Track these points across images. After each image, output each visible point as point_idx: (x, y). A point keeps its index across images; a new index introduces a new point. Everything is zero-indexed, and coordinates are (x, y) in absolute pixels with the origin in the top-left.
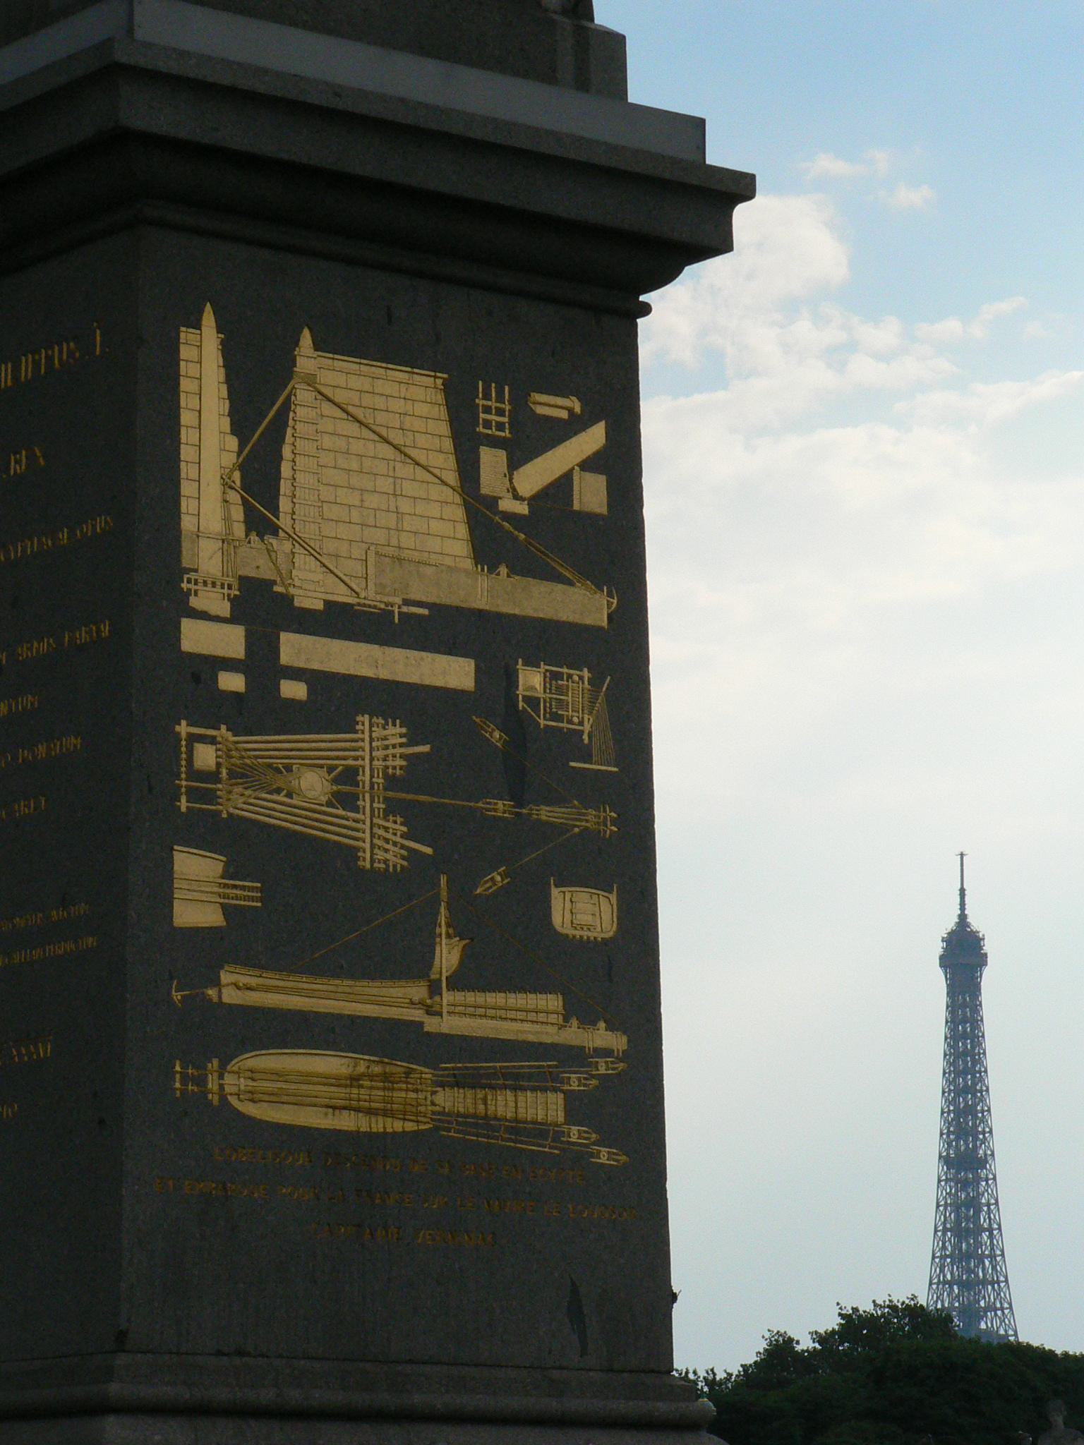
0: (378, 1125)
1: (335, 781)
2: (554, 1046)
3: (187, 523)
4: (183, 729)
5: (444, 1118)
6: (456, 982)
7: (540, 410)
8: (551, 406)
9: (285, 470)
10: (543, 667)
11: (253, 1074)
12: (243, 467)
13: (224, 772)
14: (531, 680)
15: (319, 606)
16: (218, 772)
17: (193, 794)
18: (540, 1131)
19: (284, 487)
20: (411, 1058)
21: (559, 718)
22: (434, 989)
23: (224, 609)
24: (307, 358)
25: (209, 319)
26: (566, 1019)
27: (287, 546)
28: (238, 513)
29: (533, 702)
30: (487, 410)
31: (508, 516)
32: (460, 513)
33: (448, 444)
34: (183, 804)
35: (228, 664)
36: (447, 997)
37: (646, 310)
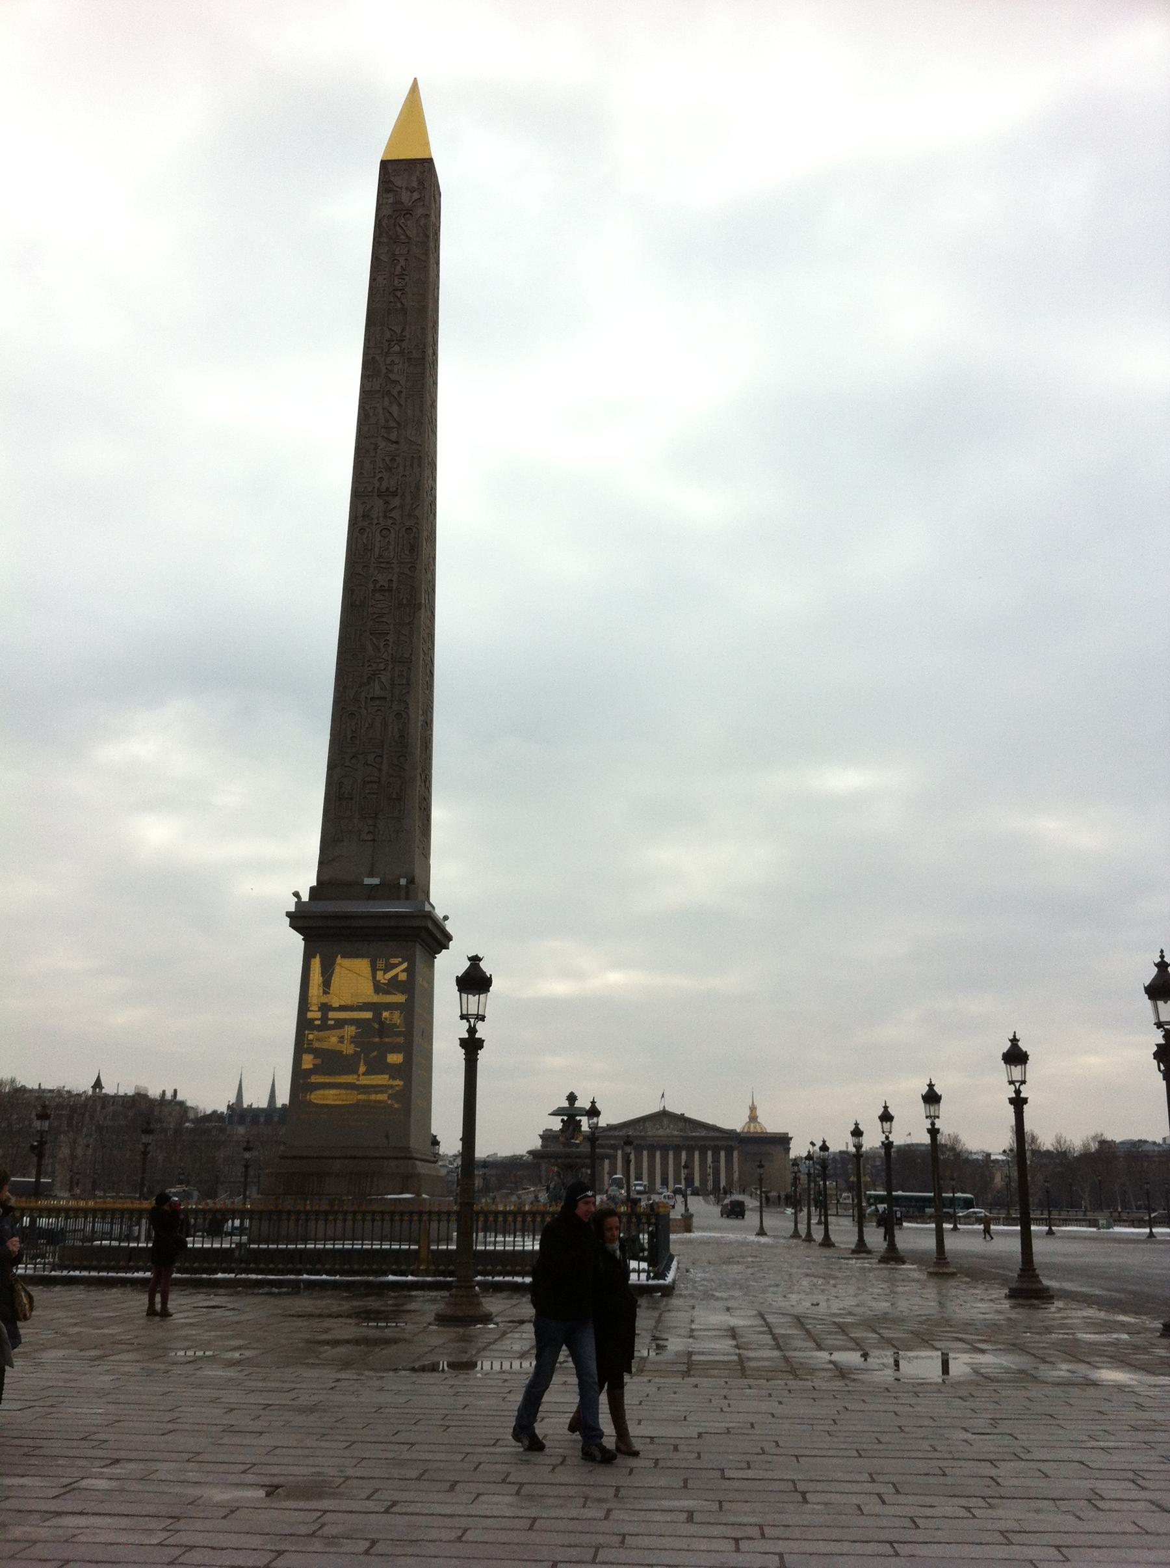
0: (344, 1103)
3: (310, 995)
4: (306, 1032)
5: (359, 1101)
6: (363, 1074)
8: (394, 961)
12: (323, 982)
14: (385, 1014)
18: (380, 1102)
22: (359, 1076)
23: (317, 1009)
24: (339, 960)
25: (318, 955)
28: (321, 991)
29: (386, 1019)
33: (370, 972)
36: (361, 1077)
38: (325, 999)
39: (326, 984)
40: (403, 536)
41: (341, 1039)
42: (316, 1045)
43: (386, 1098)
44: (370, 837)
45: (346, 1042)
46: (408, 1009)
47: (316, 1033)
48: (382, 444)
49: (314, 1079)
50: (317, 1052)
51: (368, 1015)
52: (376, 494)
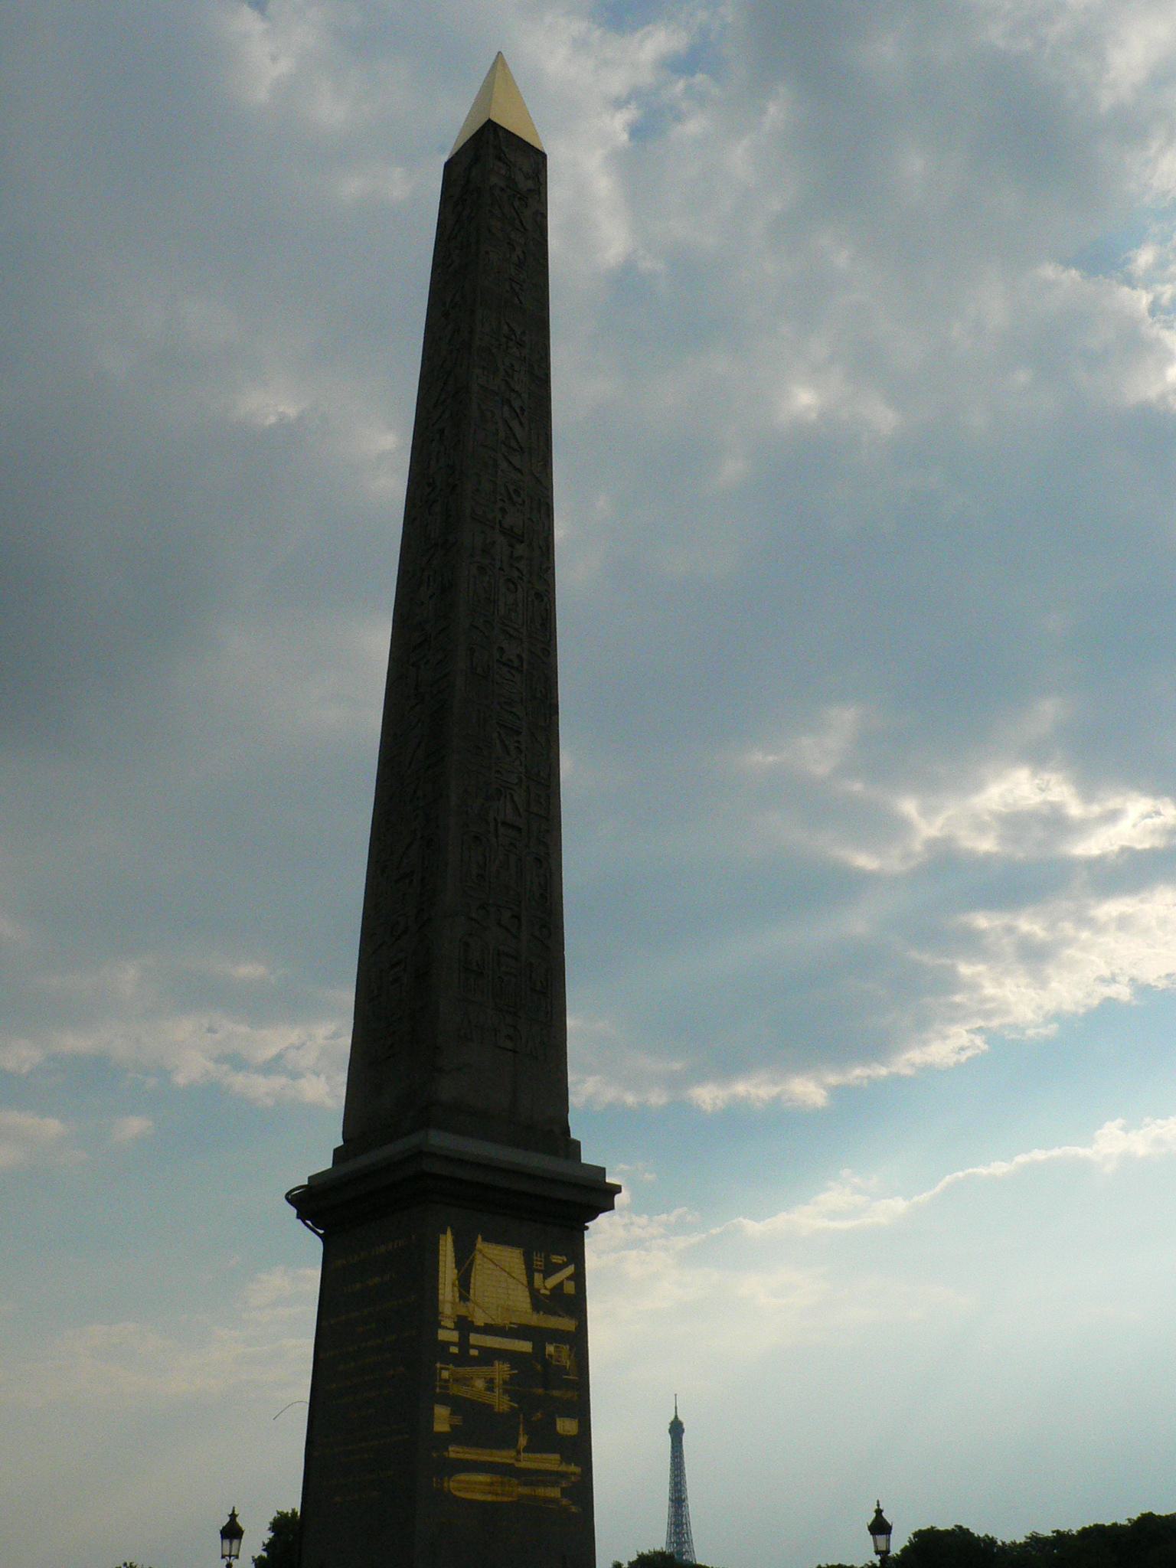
0: (499, 1499)
1: (487, 1382)
2: (557, 1472)
3: (441, 1297)
4: (438, 1365)
6: (527, 1450)
7: (554, 1261)
8: (557, 1259)
9: (472, 1281)
10: (554, 1344)
11: (459, 1482)
12: (459, 1279)
13: (451, 1380)
14: (550, 1349)
15: (483, 1324)
16: (449, 1380)
17: (440, 1388)
19: (472, 1286)
20: (511, 1476)
21: (559, 1361)
22: (518, 1453)
24: (480, 1244)
26: (561, 1463)
27: (473, 1305)
29: (550, 1356)
30: (537, 1260)
31: (543, 1294)
32: (528, 1294)
34: (438, 1390)
35: (454, 1344)
37: (587, 1228)
38: (463, 1312)
39: (464, 1283)
40: (533, 601)
41: (490, 1384)
42: (456, 1390)
43: (559, 1496)
44: (509, 1045)
45: (496, 1390)
46: (578, 1341)
47: (451, 1366)
48: (504, 465)
49: (454, 1452)
50: (458, 1405)
51: (525, 1346)
52: (498, 526)
